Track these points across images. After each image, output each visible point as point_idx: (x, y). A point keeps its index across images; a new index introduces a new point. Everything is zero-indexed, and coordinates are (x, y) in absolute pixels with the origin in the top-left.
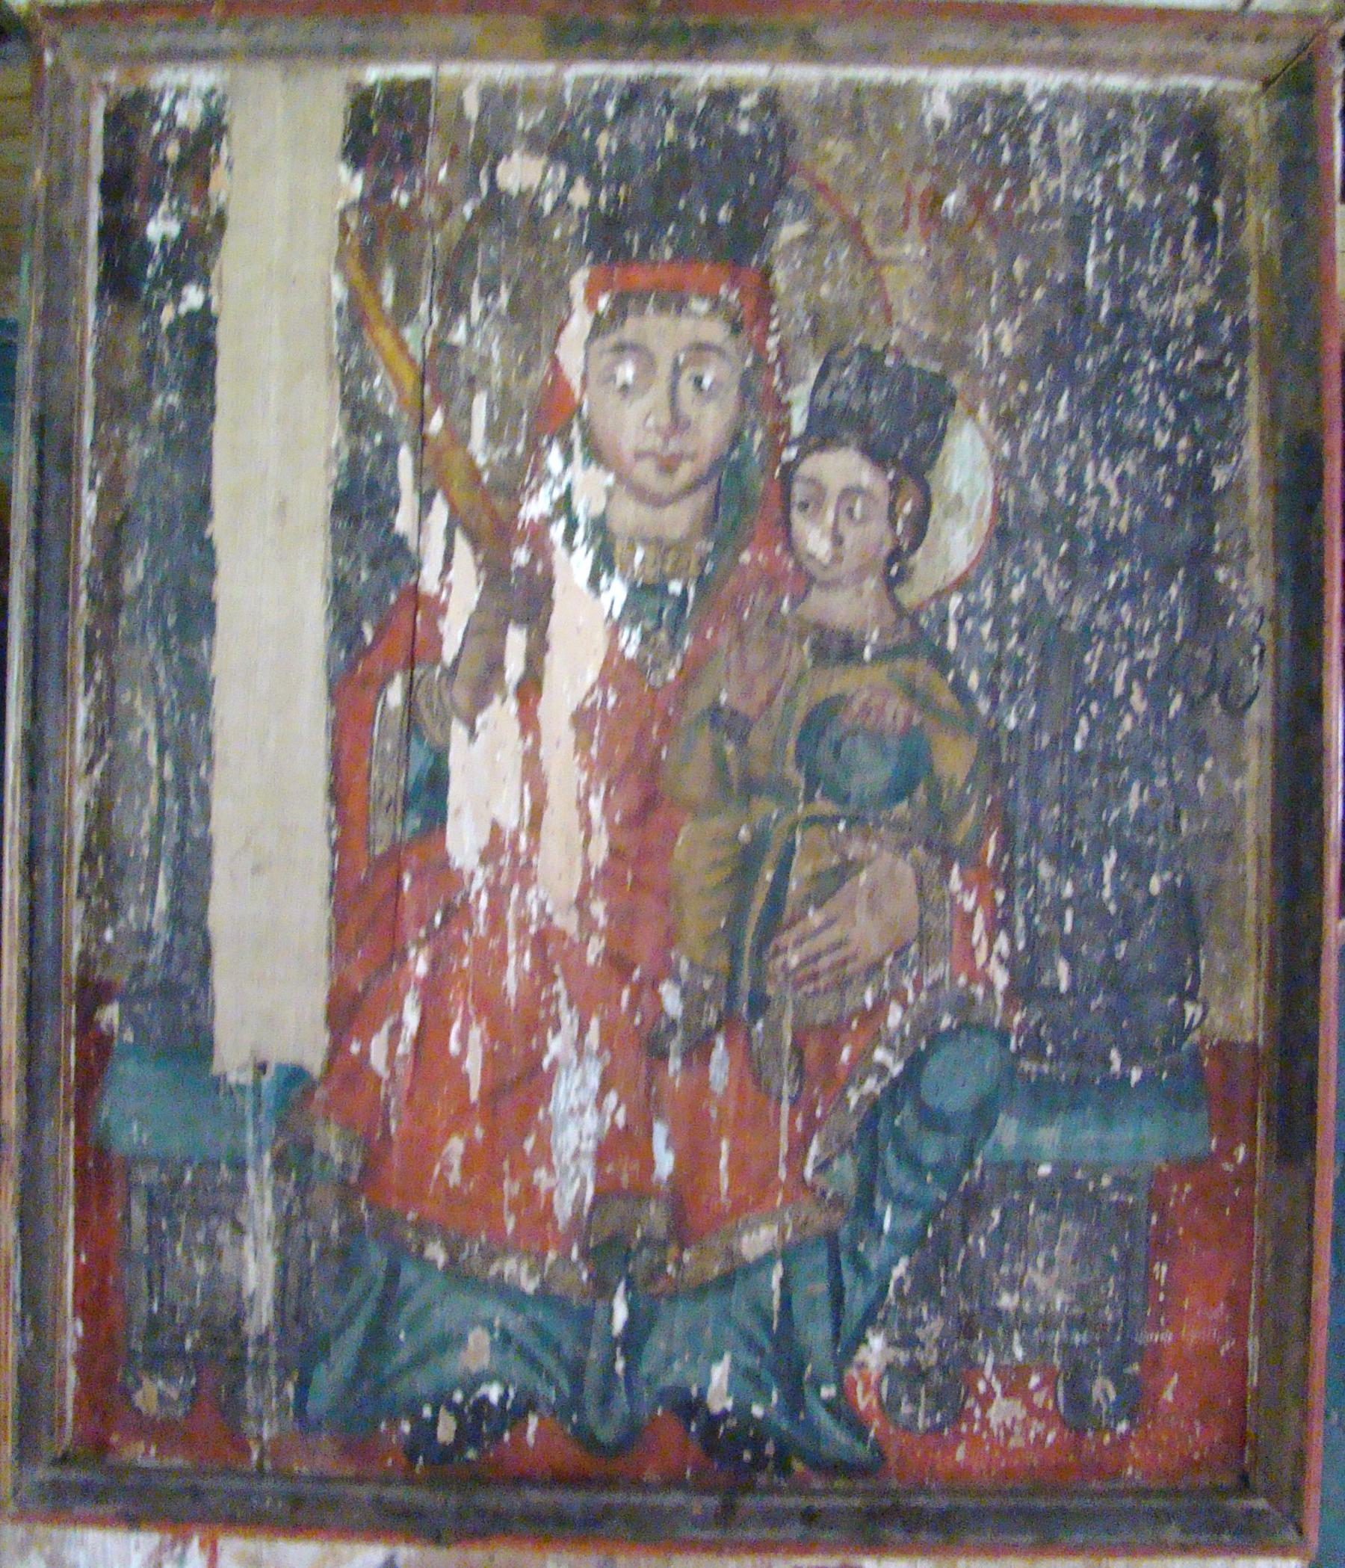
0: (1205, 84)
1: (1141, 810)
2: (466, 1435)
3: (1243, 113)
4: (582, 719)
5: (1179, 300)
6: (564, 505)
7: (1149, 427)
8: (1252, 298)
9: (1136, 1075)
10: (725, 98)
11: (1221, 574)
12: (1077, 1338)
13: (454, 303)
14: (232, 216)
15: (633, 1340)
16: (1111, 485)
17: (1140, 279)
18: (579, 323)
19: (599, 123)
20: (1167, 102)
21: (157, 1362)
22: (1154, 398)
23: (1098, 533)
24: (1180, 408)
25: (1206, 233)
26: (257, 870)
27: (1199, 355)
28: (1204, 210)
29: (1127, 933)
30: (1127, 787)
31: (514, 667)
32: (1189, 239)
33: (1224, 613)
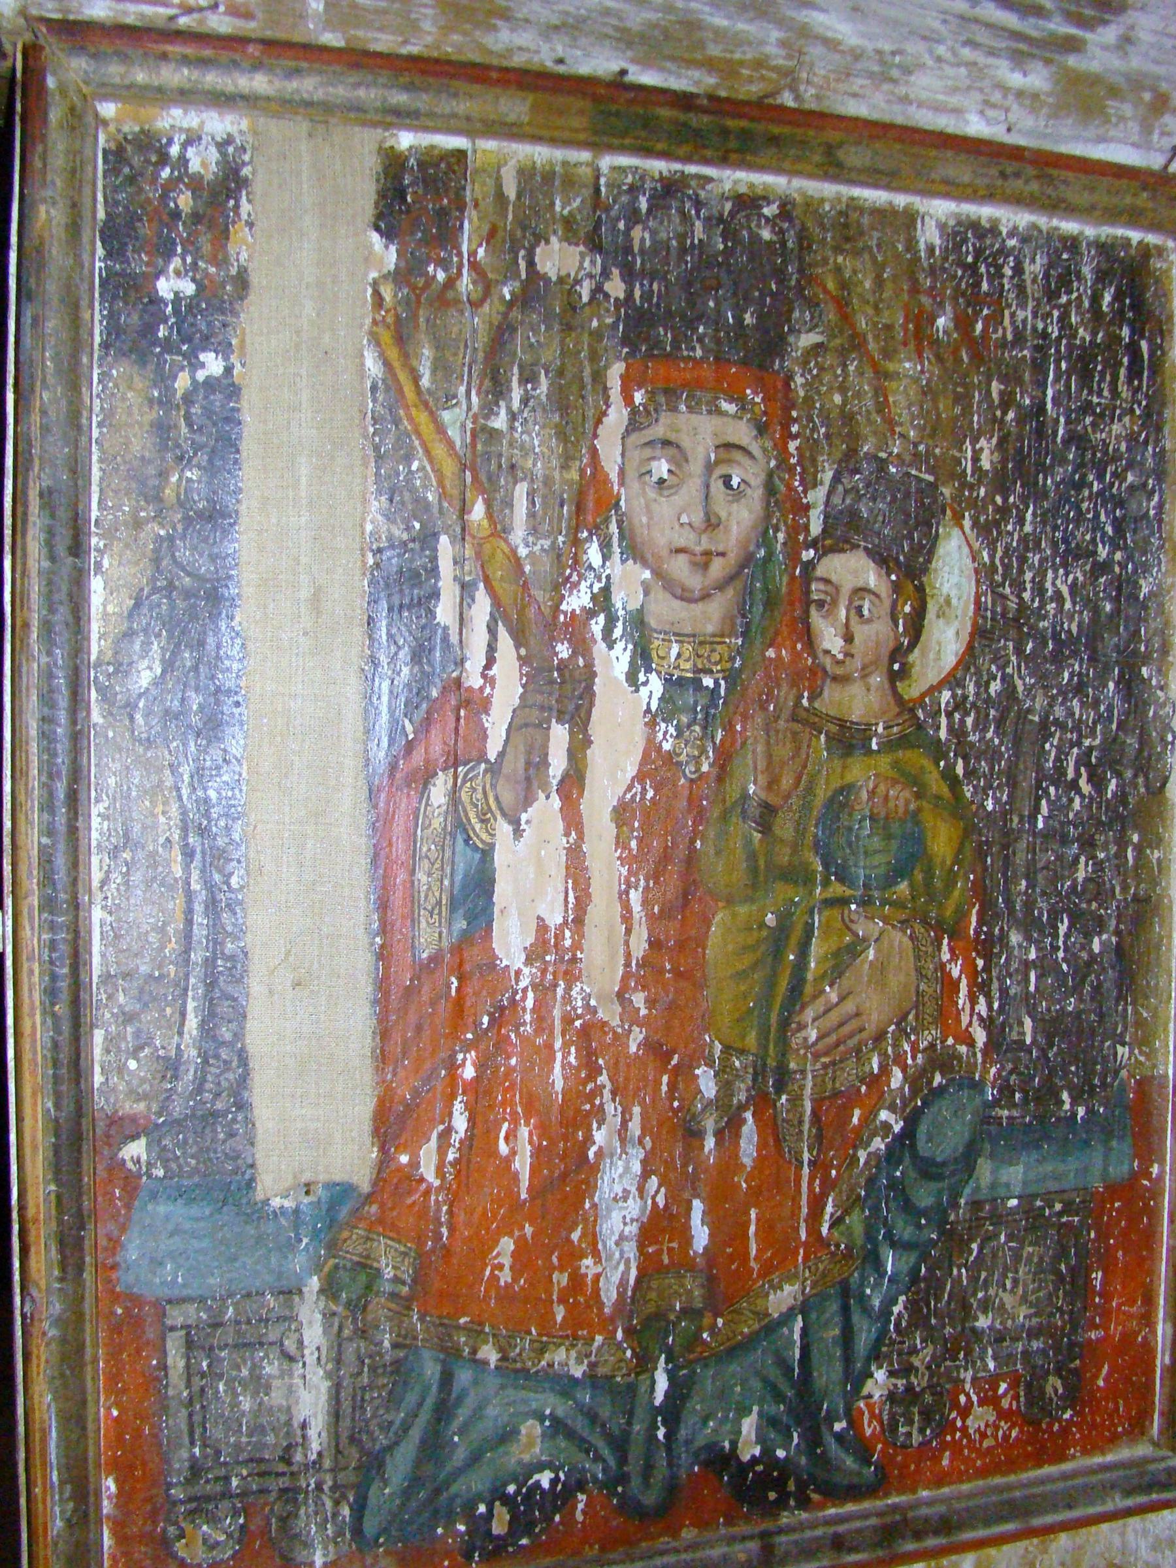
0: (1135, 236)
1: (1087, 880)
2: (520, 1525)
4: (622, 813)
5: (1116, 428)
6: (602, 601)
9: (1081, 1111)
10: (748, 203)
11: (1145, 671)
12: (1035, 1345)
13: (497, 389)
14: (254, 279)
15: (672, 1411)
16: (1065, 590)
18: (617, 416)
19: (634, 216)
20: (1104, 248)
21: (200, 1507)
22: (1097, 516)
23: (1055, 636)
24: (1118, 525)
25: (1135, 372)
26: (297, 984)
28: (1134, 350)
29: (1077, 990)
30: (1076, 860)
31: (558, 765)
32: (1123, 372)
33: (1147, 704)
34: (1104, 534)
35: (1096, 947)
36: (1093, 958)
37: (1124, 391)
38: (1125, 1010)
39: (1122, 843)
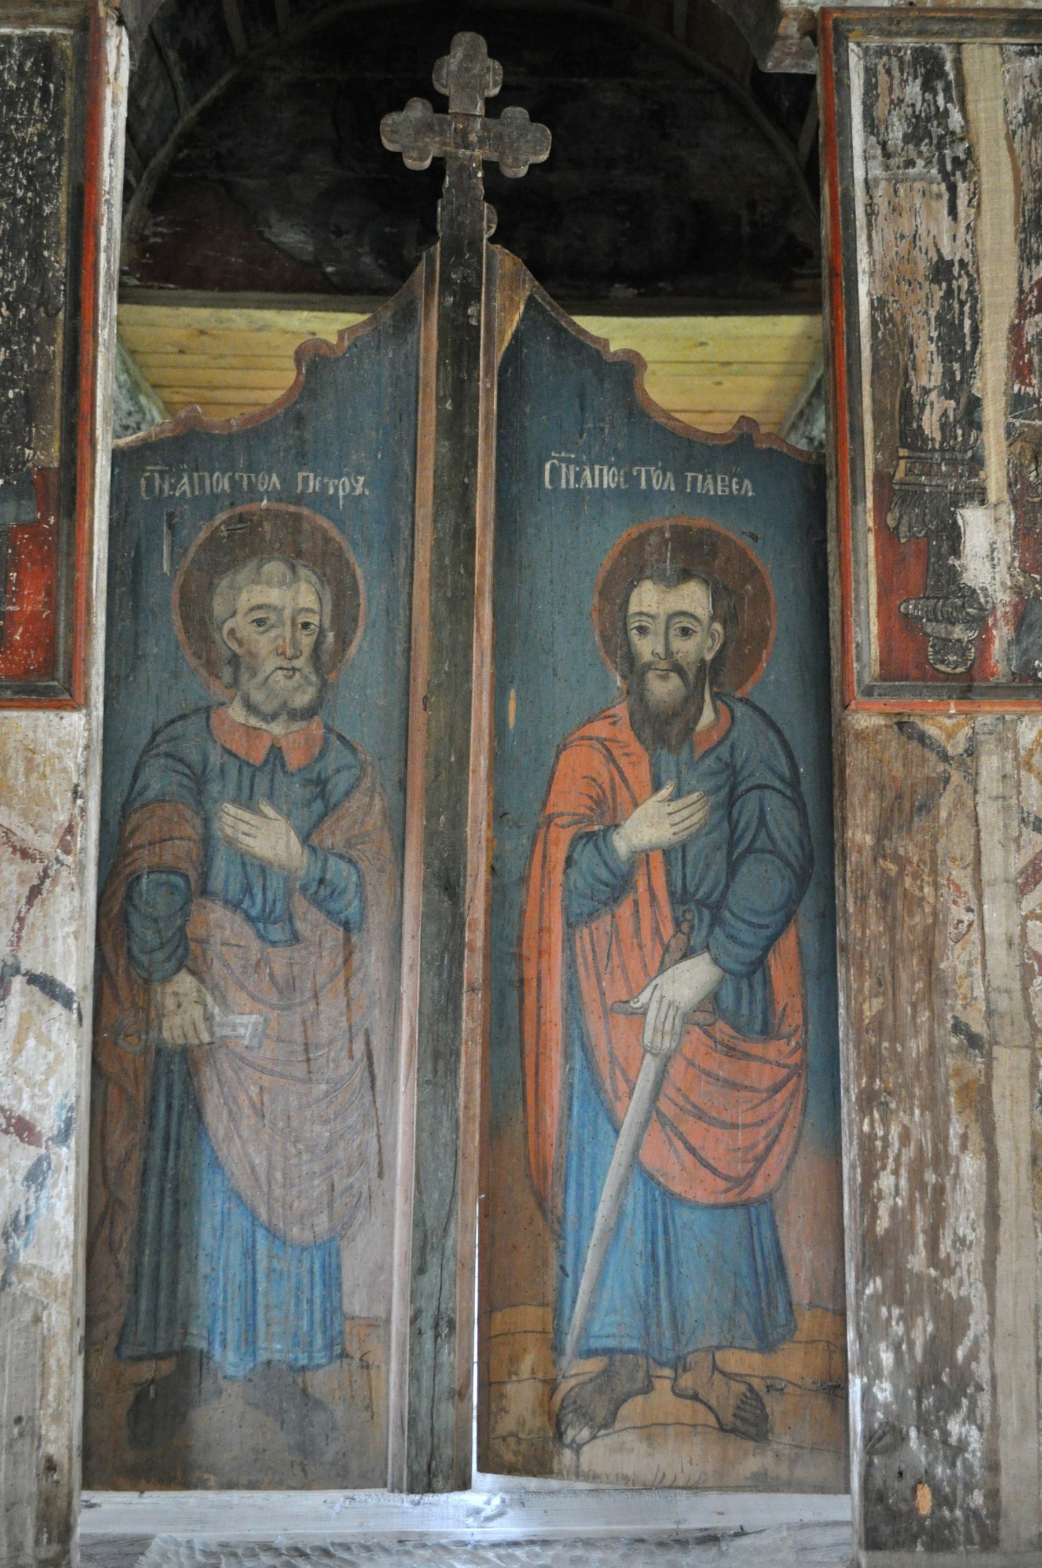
0: (48, 30)
3: (66, 44)
5: (30, 130)
7: (14, 188)
8: (66, 129)
11: (46, 253)
17: (13, 120)
20: (27, 39)
22: (17, 175)
24: (30, 179)
25: (45, 99)
27: (39, 154)
28: (45, 90)
32: (36, 102)
33: (46, 270)
34: (21, 184)
35: (11, 394)
36: (9, 401)
37: (37, 111)
38: (30, 431)
39: (30, 342)
